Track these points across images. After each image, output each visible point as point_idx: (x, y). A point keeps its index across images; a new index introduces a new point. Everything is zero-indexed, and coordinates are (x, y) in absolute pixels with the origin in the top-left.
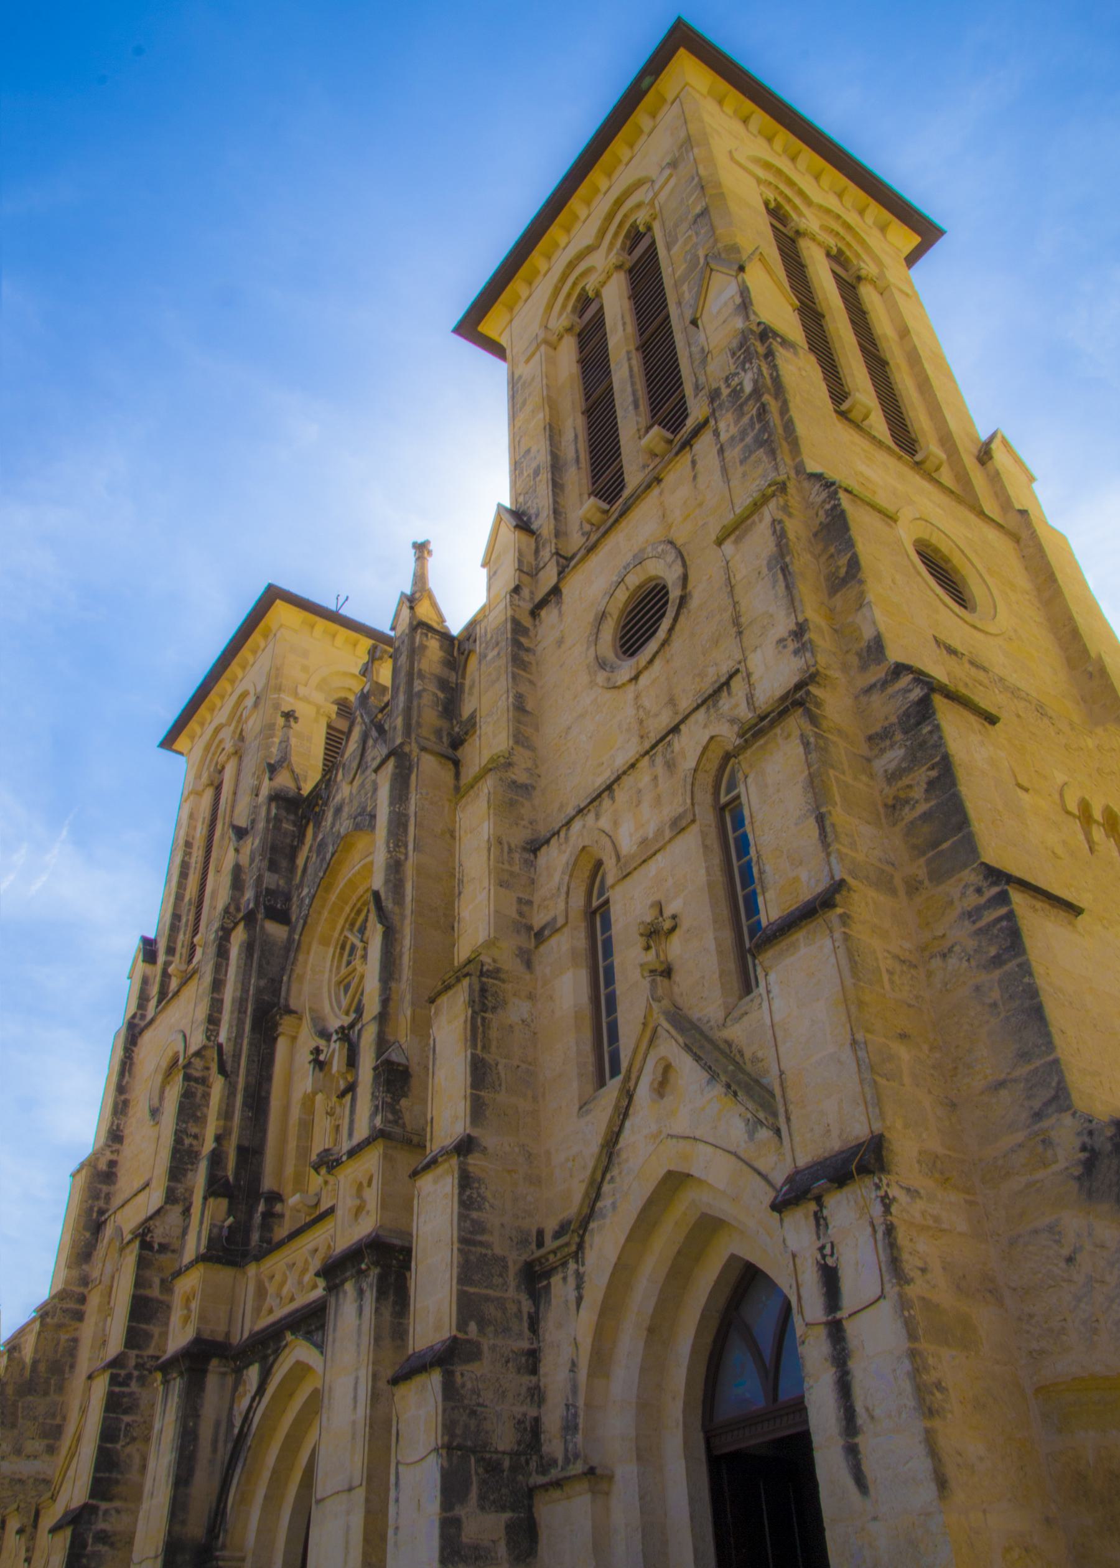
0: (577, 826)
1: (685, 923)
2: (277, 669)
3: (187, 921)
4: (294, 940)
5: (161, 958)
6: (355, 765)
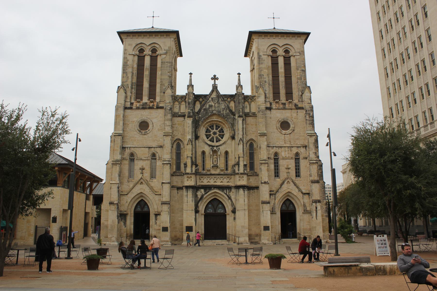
0: (275, 148)
1: (291, 169)
2: (172, 49)
4: (199, 124)
5: (129, 94)
6: (217, 101)
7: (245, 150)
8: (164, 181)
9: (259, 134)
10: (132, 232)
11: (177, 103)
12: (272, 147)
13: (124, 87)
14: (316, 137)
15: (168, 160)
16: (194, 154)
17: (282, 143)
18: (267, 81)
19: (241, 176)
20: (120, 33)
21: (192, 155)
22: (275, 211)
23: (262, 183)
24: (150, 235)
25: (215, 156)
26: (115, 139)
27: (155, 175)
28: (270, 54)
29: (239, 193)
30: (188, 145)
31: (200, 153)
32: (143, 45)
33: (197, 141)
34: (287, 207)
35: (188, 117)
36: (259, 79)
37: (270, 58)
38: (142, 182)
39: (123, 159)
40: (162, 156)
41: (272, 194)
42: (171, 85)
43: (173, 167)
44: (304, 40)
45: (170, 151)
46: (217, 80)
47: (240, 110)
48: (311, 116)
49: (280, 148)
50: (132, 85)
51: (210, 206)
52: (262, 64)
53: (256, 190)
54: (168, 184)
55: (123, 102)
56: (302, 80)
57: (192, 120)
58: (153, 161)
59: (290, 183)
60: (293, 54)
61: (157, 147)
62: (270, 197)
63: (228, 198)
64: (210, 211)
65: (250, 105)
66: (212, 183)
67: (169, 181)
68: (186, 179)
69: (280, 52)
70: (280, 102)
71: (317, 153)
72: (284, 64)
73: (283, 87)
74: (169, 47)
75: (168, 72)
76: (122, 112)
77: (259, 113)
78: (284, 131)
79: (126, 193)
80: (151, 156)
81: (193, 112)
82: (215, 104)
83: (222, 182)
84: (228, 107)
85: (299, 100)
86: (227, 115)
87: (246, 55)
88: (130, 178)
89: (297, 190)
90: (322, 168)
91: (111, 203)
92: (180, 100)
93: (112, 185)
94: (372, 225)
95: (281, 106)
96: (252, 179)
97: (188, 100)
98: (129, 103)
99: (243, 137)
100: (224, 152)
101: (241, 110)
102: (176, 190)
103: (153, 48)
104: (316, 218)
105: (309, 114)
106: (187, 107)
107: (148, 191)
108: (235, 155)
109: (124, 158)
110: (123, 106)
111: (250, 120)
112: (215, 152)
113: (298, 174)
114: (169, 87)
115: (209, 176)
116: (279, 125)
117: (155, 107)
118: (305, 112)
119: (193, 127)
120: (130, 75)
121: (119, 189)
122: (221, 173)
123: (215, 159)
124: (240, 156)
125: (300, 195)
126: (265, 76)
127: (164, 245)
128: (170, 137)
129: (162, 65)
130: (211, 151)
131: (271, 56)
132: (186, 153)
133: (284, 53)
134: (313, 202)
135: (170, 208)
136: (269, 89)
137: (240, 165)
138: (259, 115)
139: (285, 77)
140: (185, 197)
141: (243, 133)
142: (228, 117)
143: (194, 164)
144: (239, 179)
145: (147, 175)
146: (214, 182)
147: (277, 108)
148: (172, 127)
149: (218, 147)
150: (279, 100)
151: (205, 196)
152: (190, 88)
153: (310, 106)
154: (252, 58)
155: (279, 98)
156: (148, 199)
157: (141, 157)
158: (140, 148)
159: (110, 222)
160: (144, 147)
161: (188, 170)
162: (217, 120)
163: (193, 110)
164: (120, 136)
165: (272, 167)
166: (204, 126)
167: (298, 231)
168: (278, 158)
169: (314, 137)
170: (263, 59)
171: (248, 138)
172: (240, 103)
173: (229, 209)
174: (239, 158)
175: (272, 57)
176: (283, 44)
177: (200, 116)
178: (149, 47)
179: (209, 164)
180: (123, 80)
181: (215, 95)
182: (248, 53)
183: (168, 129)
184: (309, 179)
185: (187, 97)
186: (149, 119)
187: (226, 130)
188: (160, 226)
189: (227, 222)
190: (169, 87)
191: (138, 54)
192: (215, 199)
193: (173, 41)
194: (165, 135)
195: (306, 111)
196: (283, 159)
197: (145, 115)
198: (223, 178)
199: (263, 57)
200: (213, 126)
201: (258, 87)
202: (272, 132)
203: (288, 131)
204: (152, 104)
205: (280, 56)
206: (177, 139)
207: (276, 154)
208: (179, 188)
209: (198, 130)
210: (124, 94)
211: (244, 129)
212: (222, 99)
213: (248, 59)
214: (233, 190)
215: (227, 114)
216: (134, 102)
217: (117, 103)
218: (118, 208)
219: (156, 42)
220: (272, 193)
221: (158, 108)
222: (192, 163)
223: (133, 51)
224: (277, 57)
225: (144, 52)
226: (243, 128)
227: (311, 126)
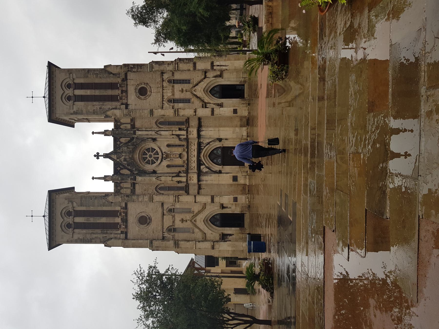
0: (164, 102)
1: (183, 87)
3: (106, 230)
5: (112, 236)
6: (120, 154)
7: (166, 129)
8: (194, 201)
9: (151, 116)
10: (238, 228)
11: (122, 191)
12: (163, 104)
13: (106, 241)
14: (153, 63)
15: (175, 197)
16: (169, 175)
17: (160, 95)
18: (99, 107)
19: (189, 133)
20: (50, 248)
21: (170, 176)
22: (221, 104)
23: (196, 115)
24: (240, 212)
25: (172, 156)
26: (155, 246)
27: (188, 209)
28: (72, 102)
29: (204, 135)
30: (162, 180)
31: (169, 169)
32: (63, 224)
33: (157, 172)
34: (217, 93)
35: (136, 181)
36: (97, 114)
37: (76, 103)
38: (195, 221)
39: (173, 239)
40: (171, 203)
41: (205, 105)
42: (104, 196)
43: (181, 193)
44: (56, 69)
45: (167, 196)
46: (99, 153)
47: (129, 133)
48: (134, 66)
49: (164, 97)
50: (104, 233)
51: (215, 161)
52: (82, 111)
53: (202, 120)
54: (196, 197)
55: (120, 241)
56: (98, 72)
57: (139, 177)
58: (175, 211)
59: (195, 90)
60: (72, 80)
61: (163, 208)
62: (207, 108)
63: (209, 145)
64: (219, 160)
65: (124, 124)
66: (195, 159)
67: (194, 198)
68: (192, 182)
69: (69, 92)
70: (120, 95)
71: (168, 62)
72: (82, 89)
73: (105, 92)
74: (65, 200)
75: (91, 199)
76: (129, 241)
77: (131, 115)
78: (148, 93)
79: (204, 235)
80: (171, 213)
81: (131, 176)
82: (123, 156)
83: (194, 150)
84: (126, 143)
85: (118, 77)
86: (133, 145)
87: (73, 126)
89: (202, 83)
90: (182, 58)
91: (213, 248)
92: (119, 188)
93: (197, 247)
94: (235, 12)
95: (124, 94)
96: (192, 123)
97: (119, 180)
98: (122, 235)
99: (154, 131)
100: (167, 148)
101: (128, 132)
102: (202, 190)
103: (66, 214)
104: (227, 66)
105: (131, 68)
106: (126, 181)
107: (202, 214)
108: (171, 138)
109: (173, 238)
110: (124, 241)
111: (138, 124)
112: (167, 156)
113: (187, 82)
114: (106, 199)
115: (189, 161)
116: (143, 97)
117: (126, 210)
118: (130, 72)
119: (145, 176)
120: (94, 236)
121: (200, 241)
122: (186, 150)
123: (174, 156)
124: (171, 134)
125: (207, 81)
126: (95, 109)
127: (249, 200)
128: (154, 196)
129: (84, 206)
130: (166, 159)
131: (74, 102)
132: (169, 182)
133: (71, 88)
134: (213, 69)
135: (217, 196)
136: (108, 105)
138: (133, 115)
139: (95, 89)
140: (207, 182)
141: (150, 130)
142: (135, 144)
143: (179, 175)
144: (192, 135)
145: (188, 216)
146: (195, 157)
147: (126, 99)
148: (144, 195)
149: (164, 153)
150: (118, 96)
151: (207, 165)
152: (107, 178)
153: (124, 66)
154: (75, 120)
155: (117, 96)
156: (209, 215)
157: (172, 222)
158: (164, 223)
159: (230, 249)
160: (163, 219)
161: (184, 179)
162: (138, 154)
163: (129, 176)
164: (153, 242)
165: (181, 105)
166: (144, 166)
167: (238, 83)
168: (173, 99)
169: (153, 64)
171: (155, 126)
172: (122, 133)
173: (218, 144)
174: (173, 135)
175: (75, 101)
176: (62, 89)
177: (134, 169)
178: (65, 218)
179: (179, 161)
180: (99, 242)
182: (71, 124)
183: (146, 198)
184: (192, 71)
185: (116, 181)
186: (137, 216)
187: (147, 146)
188: (232, 204)
189: (230, 146)
190: (106, 199)
191: (72, 229)
192: (209, 156)
193: (59, 196)
194: (152, 201)
195: (129, 71)
196: (173, 95)
197: (132, 219)
198: (191, 149)
199: (75, 109)
200: (144, 158)
201: (106, 115)
202: (149, 104)
203: (147, 89)
204: (122, 213)
205: (73, 93)
206: (156, 190)
207: (170, 101)
208: (200, 188)
209: (148, 171)
210: (113, 240)
211: (146, 129)
212: (118, 149)
213: (76, 124)
214: (201, 141)
216: (120, 231)
217: (121, 246)
218: (217, 241)
219: (60, 212)
220: (204, 106)
221: (126, 207)
222: (178, 176)
223: (69, 234)
224: (75, 96)
225: (71, 223)
226: (146, 131)
227: (143, 67)
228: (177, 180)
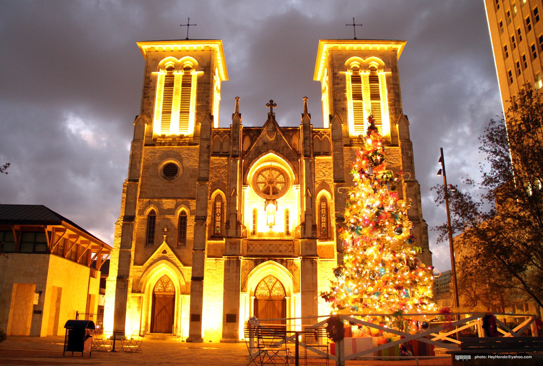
52: (338, 84)
71: (419, 209)
88: (149, 243)
97: (233, 134)
105: (407, 154)
114: (206, 116)
137: (307, 227)
170: (340, 78)
181: (272, 127)
215: (289, 154)
228: (230, 222)
